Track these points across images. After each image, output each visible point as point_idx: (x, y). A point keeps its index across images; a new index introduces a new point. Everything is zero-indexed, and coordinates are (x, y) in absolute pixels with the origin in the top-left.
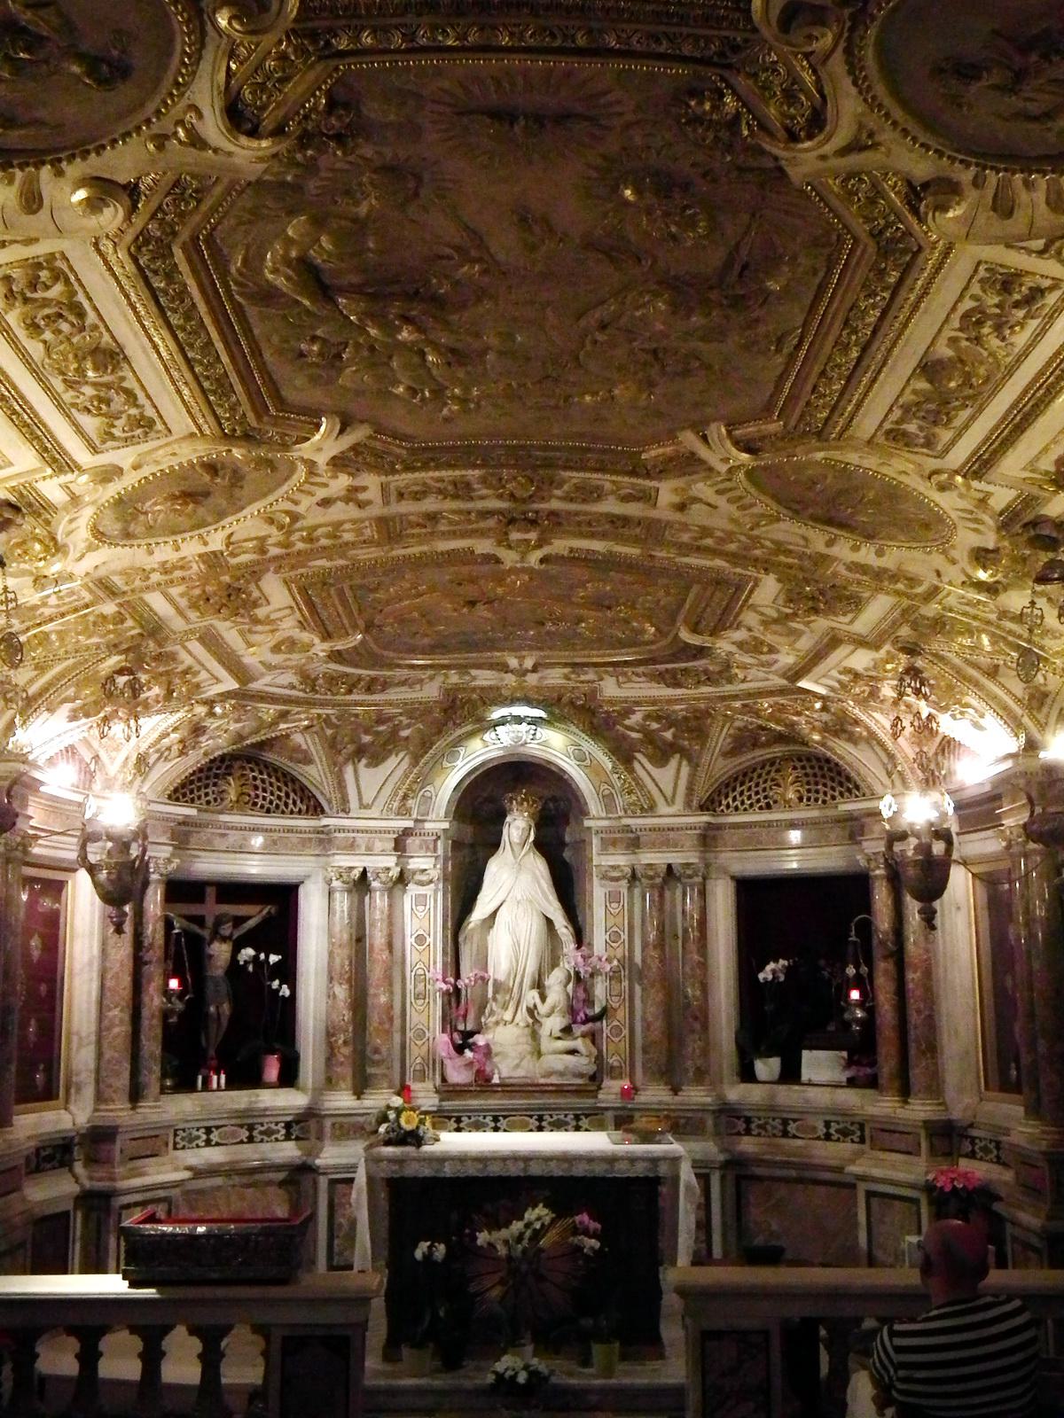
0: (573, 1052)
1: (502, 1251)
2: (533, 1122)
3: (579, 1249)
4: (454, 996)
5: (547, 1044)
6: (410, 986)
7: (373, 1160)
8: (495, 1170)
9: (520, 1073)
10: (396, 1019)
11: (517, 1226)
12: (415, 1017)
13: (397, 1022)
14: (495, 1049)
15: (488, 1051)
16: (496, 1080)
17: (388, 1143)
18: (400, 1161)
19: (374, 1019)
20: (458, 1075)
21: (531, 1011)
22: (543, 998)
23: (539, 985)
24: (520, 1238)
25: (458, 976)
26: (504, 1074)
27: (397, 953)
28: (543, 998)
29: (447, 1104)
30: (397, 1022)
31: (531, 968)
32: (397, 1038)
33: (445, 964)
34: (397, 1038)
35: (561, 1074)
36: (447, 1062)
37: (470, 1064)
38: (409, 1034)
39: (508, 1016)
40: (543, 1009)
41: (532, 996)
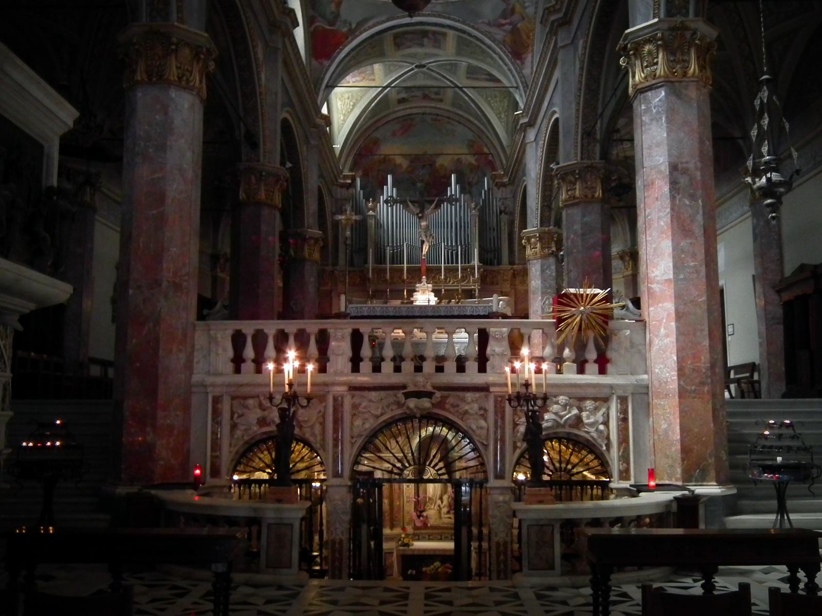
0: (450, 518)
1: (428, 572)
2: (439, 537)
3: (447, 572)
4: (417, 503)
5: (443, 516)
6: (405, 499)
7: (398, 550)
8: (427, 553)
9: (436, 523)
10: (401, 508)
11: (432, 567)
12: (406, 508)
13: (402, 509)
14: (429, 517)
15: (427, 517)
16: (429, 525)
17: (401, 546)
18: (404, 550)
19: (396, 509)
20: (418, 524)
21: (439, 506)
22: (442, 502)
23: (441, 498)
24: (433, 569)
25: (418, 496)
26: (431, 523)
27: (402, 491)
28: (442, 502)
29: (416, 532)
30: (402, 509)
31: (439, 493)
32: (402, 513)
33: (415, 493)
34: (402, 513)
35: (446, 524)
36: (416, 521)
37: (422, 521)
38: (405, 512)
39: (432, 507)
40: (442, 506)
41: (439, 502)
